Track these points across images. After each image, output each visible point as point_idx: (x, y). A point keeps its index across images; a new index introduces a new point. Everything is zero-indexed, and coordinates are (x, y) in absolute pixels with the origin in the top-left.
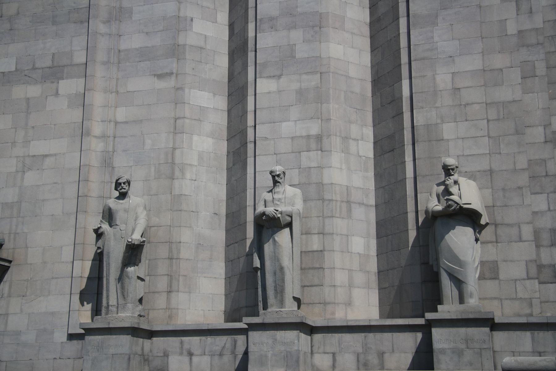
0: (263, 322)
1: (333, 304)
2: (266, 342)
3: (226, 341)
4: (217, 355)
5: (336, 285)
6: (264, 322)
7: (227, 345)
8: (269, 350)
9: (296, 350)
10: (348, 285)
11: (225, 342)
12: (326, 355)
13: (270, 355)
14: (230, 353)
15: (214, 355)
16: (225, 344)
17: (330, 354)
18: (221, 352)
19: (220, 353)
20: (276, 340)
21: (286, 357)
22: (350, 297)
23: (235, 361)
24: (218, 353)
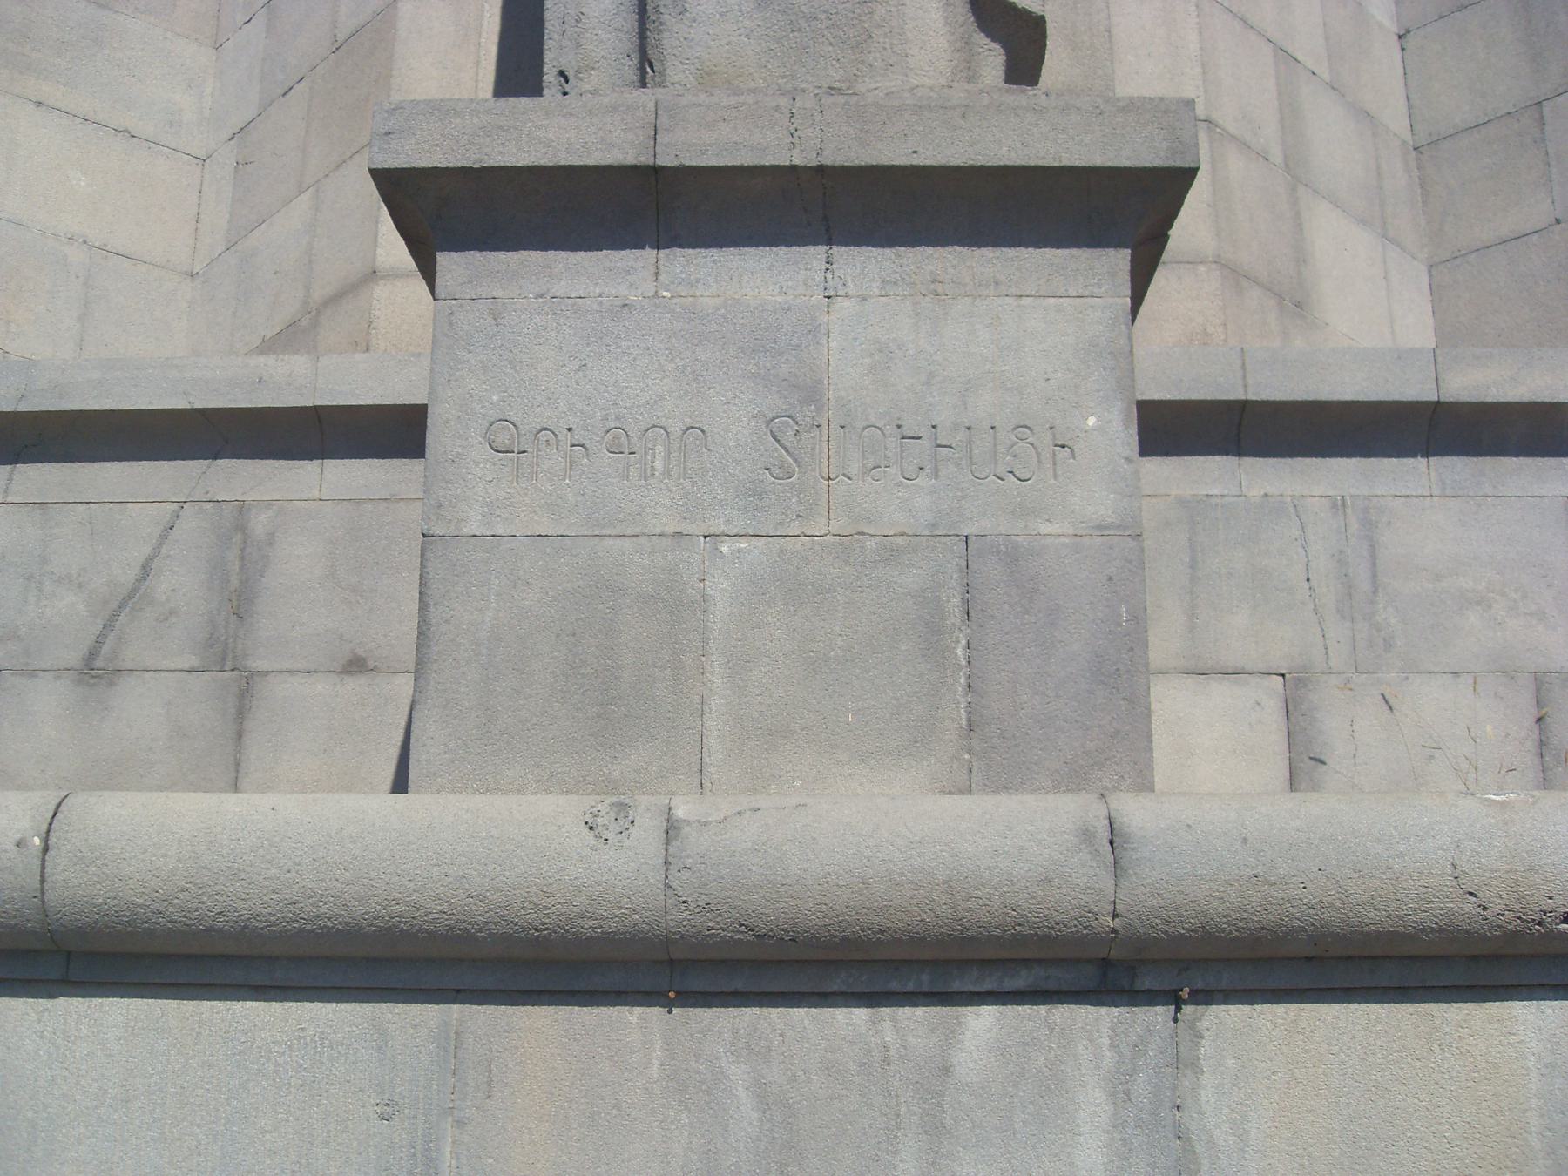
0: (645, 159)
1: (1202, 268)
2: (676, 429)
3: (163, 537)
4: (59, 672)
5: (1214, 116)
6: (666, 160)
7: (162, 586)
8: (718, 526)
9: (1101, 528)
10: (1277, 155)
11: (147, 550)
12: (1221, 693)
13: (719, 587)
14: (193, 661)
15: (32, 673)
16: (146, 569)
17: (1254, 680)
18: (99, 641)
19: (93, 654)
20: (812, 394)
21: (956, 618)
22: (1301, 257)
23: (240, 735)
24: (73, 656)
